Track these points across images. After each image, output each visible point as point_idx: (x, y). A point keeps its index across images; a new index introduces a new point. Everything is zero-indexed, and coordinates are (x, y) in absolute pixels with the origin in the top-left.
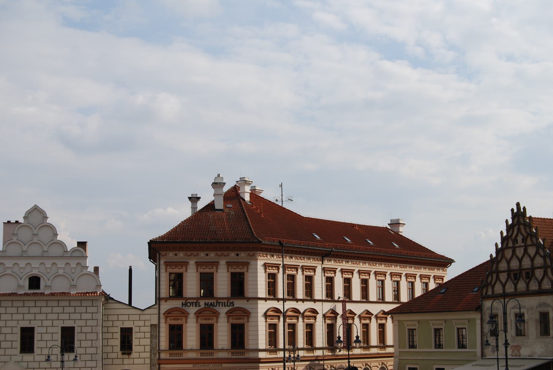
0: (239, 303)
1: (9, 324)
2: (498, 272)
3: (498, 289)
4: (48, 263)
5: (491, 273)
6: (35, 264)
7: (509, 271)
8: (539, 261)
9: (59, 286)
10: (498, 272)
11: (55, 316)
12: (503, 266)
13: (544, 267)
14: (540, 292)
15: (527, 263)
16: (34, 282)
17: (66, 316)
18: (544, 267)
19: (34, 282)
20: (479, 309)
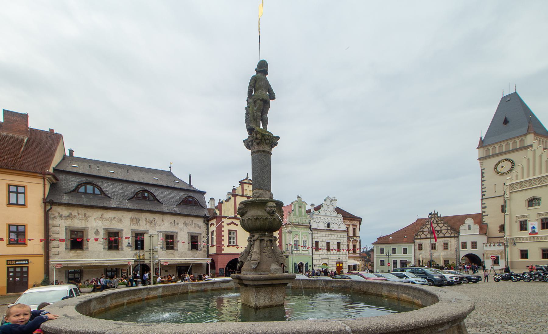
0: (355, 238)
1: (324, 240)
2: (423, 231)
3: (423, 236)
4: (333, 219)
5: (420, 232)
6: (329, 218)
7: (429, 231)
8: (444, 228)
9: (336, 227)
10: (423, 231)
11: (335, 238)
12: (426, 229)
13: (447, 230)
14: (444, 237)
15: (438, 228)
16: (329, 225)
17: (338, 238)
18: (447, 230)
19: (329, 225)
20: (414, 242)
